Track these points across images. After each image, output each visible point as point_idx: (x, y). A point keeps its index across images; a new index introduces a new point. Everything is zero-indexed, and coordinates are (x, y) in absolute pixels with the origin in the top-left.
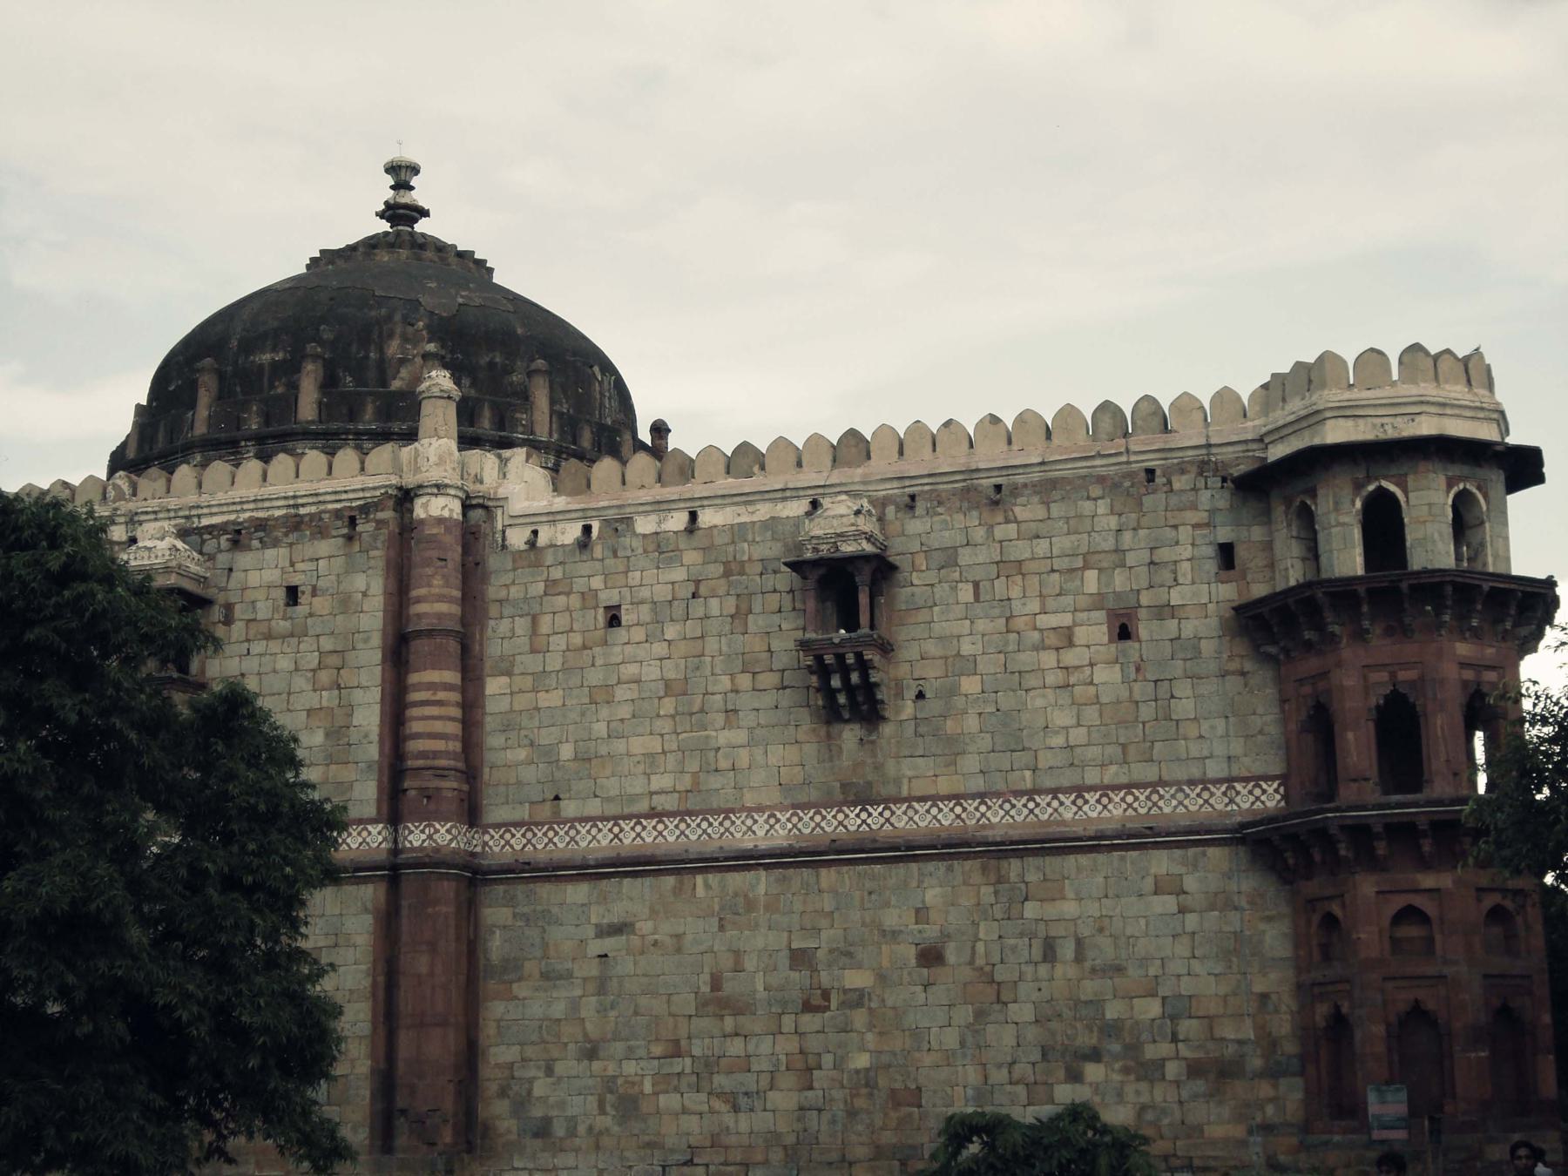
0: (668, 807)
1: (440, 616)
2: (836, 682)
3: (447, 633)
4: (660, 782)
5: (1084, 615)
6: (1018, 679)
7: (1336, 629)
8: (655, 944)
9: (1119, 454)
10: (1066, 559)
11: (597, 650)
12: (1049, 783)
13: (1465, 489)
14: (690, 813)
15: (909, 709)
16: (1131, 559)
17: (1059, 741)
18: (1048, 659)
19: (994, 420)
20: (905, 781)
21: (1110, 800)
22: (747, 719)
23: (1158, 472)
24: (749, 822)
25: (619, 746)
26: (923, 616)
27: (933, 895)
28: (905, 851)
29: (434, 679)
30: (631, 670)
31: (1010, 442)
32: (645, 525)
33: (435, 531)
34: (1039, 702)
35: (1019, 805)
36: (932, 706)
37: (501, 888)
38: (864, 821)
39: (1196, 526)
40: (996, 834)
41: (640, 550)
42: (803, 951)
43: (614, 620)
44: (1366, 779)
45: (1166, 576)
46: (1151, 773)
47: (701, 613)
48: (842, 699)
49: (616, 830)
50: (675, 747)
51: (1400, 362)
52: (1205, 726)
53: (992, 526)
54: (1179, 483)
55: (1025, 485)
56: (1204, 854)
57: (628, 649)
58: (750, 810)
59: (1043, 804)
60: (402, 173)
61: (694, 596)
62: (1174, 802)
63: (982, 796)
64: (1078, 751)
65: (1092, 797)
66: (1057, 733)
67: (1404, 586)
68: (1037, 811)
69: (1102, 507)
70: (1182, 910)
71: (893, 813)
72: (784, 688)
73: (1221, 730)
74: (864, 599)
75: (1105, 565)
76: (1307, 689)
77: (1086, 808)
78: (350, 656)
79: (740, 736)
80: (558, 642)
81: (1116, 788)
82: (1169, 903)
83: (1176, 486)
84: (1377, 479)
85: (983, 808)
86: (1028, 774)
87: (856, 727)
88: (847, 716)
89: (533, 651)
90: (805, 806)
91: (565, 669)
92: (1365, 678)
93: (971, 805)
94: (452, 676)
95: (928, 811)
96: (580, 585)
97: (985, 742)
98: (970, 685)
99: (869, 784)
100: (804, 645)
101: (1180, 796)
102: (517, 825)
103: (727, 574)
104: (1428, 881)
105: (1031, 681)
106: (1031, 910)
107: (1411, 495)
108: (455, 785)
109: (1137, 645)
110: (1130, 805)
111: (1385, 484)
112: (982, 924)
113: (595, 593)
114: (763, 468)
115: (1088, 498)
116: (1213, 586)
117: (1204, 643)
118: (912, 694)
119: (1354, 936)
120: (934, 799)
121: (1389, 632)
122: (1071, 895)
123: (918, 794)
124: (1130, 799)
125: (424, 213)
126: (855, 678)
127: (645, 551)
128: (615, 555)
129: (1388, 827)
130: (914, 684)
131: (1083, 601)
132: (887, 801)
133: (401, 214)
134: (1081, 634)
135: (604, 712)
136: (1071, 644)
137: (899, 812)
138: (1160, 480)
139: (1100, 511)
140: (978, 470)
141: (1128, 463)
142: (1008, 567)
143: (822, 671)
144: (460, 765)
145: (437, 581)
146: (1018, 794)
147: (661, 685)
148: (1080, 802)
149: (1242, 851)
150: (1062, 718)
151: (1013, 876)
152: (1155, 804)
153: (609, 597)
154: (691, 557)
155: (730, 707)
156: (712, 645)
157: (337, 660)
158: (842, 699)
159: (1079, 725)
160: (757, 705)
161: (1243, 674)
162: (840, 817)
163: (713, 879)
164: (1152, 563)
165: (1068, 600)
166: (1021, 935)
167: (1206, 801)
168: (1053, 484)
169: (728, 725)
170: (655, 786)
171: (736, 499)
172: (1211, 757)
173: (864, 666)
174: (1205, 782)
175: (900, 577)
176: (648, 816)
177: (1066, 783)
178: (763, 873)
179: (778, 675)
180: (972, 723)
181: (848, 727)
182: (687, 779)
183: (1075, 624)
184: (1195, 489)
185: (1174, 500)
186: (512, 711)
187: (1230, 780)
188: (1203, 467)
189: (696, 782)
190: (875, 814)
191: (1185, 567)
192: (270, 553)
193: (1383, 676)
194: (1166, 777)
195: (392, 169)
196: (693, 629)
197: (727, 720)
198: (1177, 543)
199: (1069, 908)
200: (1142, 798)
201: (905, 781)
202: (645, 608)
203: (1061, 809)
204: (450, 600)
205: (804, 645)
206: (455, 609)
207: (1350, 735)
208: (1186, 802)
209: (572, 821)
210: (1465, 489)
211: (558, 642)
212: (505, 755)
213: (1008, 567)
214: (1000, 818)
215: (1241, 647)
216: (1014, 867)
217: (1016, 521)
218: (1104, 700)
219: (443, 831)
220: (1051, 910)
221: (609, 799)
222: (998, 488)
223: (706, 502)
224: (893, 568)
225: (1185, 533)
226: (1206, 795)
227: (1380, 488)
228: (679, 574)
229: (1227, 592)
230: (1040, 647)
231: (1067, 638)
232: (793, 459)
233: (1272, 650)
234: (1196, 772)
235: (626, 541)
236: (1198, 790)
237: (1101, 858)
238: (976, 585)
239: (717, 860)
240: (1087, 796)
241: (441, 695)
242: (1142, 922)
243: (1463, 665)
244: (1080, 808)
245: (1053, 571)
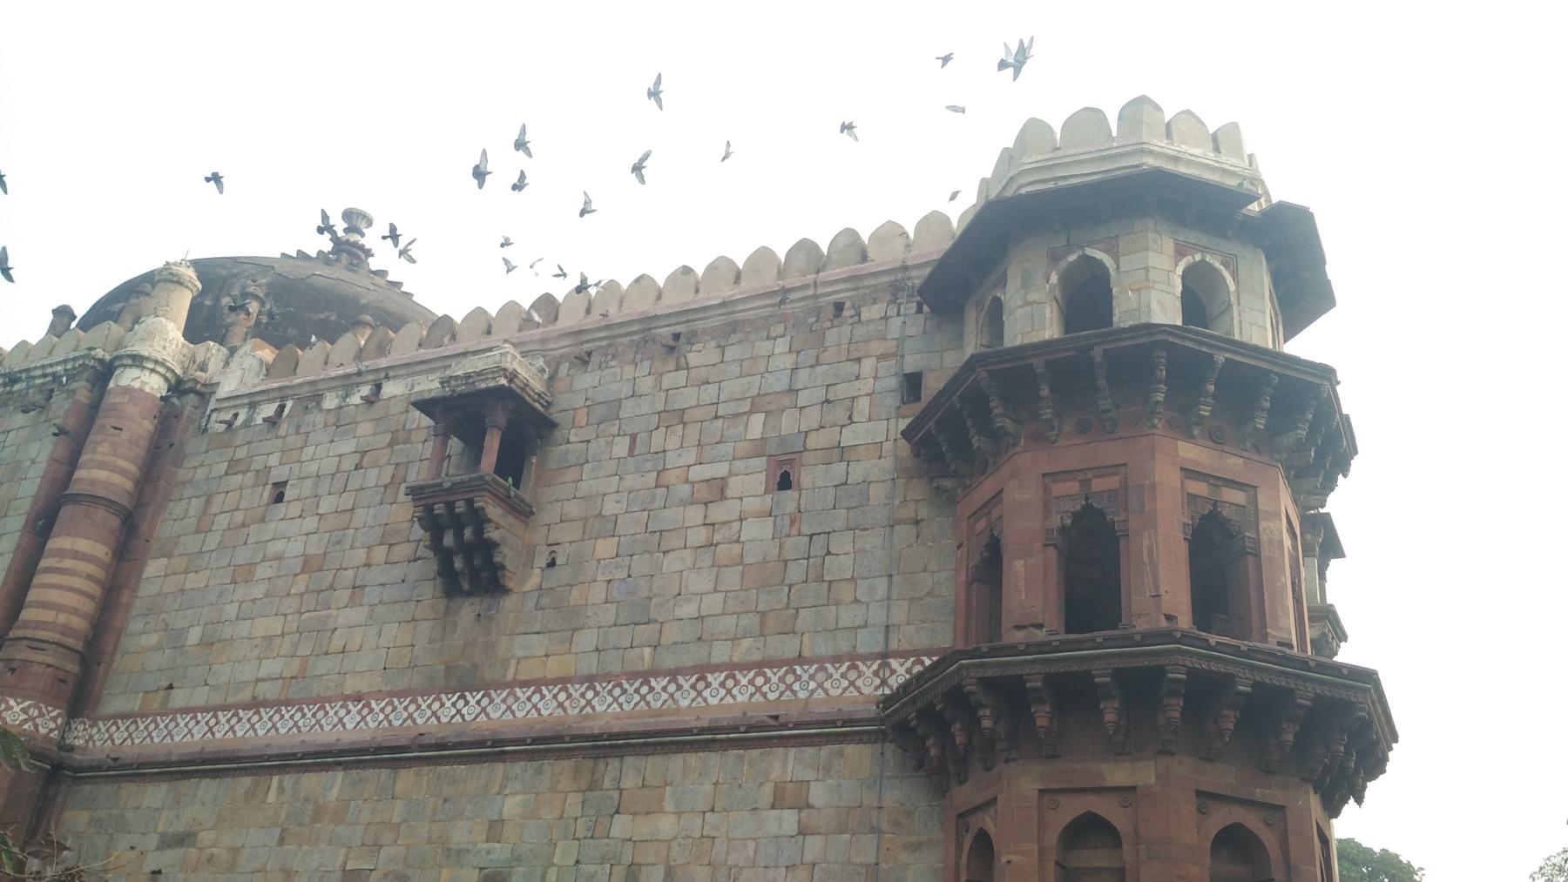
0: (270, 696)
1: (93, 482)
2: (448, 540)
3: (109, 503)
4: (271, 667)
5: (739, 465)
6: (658, 540)
7: (1009, 425)
8: (210, 859)
9: (805, 287)
10: (733, 404)
12: (670, 662)
13: (1203, 261)
14: (288, 703)
15: (534, 579)
16: (803, 399)
17: (687, 610)
18: (695, 514)
19: (686, 270)
20: (514, 662)
21: (737, 683)
22: (372, 595)
23: (848, 304)
24: (342, 712)
25: (244, 628)
26: (571, 475)
27: (511, 806)
28: (490, 749)
29: (80, 550)
30: (276, 547)
31: (697, 291)
32: (330, 402)
33: (118, 400)
34: (677, 566)
35: (631, 690)
36: (562, 574)
37: (87, 788)
38: (459, 711)
39: (880, 358)
40: (595, 727)
42: (356, 872)
43: (279, 498)
44: (1039, 626)
45: (840, 415)
46: (789, 647)
47: (357, 486)
48: (458, 564)
49: (213, 722)
50: (295, 626)
51: (1121, 117)
52: (863, 586)
53: (661, 375)
54: (871, 312)
55: (704, 331)
56: (841, 754)
57: (283, 524)
58: (346, 698)
59: (658, 688)
61: (357, 467)
62: (813, 685)
63: (591, 680)
64: (710, 621)
65: (715, 679)
66: (688, 601)
67: (1097, 354)
68: (649, 698)
69: (781, 345)
70: (803, 832)
71: (492, 701)
73: (881, 592)
74: (493, 443)
75: (773, 407)
76: (981, 524)
77: (706, 693)
79: (357, 614)
80: (222, 522)
81: (745, 667)
82: (789, 820)
83: (865, 316)
84: (1082, 248)
85: (590, 695)
86: (648, 651)
87: (475, 600)
88: (466, 587)
89: (198, 531)
90: (401, 694)
91: (221, 546)
92: (1046, 490)
93: (576, 690)
94: (102, 551)
95: (529, 699)
96: (258, 464)
97: (609, 614)
98: (605, 548)
99: (476, 666)
100: (415, 492)
101: (821, 676)
102: (124, 717)
103: (391, 444)
104: (1117, 774)
105: (672, 541)
106: (621, 826)
107: (1123, 260)
108: (50, 660)
109: (796, 495)
110: (758, 689)
111: (1089, 252)
112: (560, 843)
113: (268, 469)
114: (453, 337)
115: (768, 338)
116: (893, 421)
117: (873, 489)
118: (541, 561)
119: (1004, 860)
120: (538, 684)
121: (1083, 428)
122: (669, 805)
123: (522, 677)
124: (760, 681)
126: (468, 533)
127: (326, 426)
128: (298, 427)
129: (1050, 679)
130: (546, 551)
131: (743, 448)
132: (486, 687)
134: (735, 486)
135: (241, 592)
136: (723, 496)
137: (498, 700)
138: (846, 313)
139: (777, 351)
140: (656, 317)
141: (815, 297)
142: (675, 417)
143: (433, 524)
144: (79, 646)
145: (104, 448)
146: (631, 676)
147: (300, 561)
148: (701, 685)
149: (890, 748)
150: (698, 582)
151: (607, 784)
152: (789, 687)
153: (278, 474)
154: (365, 429)
155: (359, 582)
156: (360, 516)
158: (458, 564)
159: (715, 591)
160: (383, 580)
161: (917, 522)
162: (436, 705)
163: (289, 780)
164: (827, 401)
165: (727, 448)
166: (603, 860)
167: (852, 683)
168: (734, 327)
169: (352, 603)
170: (263, 673)
171: (419, 368)
172: (865, 626)
173: (479, 519)
174: (854, 658)
175: (557, 434)
176: (246, 707)
177: (688, 661)
178: (340, 775)
180: (598, 593)
182: (297, 661)
183: (731, 474)
184: (886, 318)
185: (860, 331)
186: (160, 594)
187: (885, 656)
188: (896, 289)
189: (304, 668)
190: (473, 702)
191: (863, 403)
193: (1073, 487)
194: (806, 653)
196: (347, 500)
197: (352, 597)
198: (858, 378)
199: (666, 825)
200: (775, 679)
201: (514, 662)
202: (309, 482)
203: (677, 695)
204: (123, 472)
205: (415, 492)
206: (128, 485)
207: (1019, 565)
208: (827, 685)
209: (175, 712)
210: (1203, 261)
211: (222, 522)
212: (140, 639)
213: (675, 417)
214: (608, 708)
215: (918, 489)
216: (610, 769)
217: (688, 368)
218: (748, 560)
219: (17, 709)
220: (643, 828)
221: (217, 688)
222: (677, 337)
224: (552, 425)
225: (868, 365)
226: (853, 675)
227: (1085, 258)
228: (348, 446)
229: (904, 424)
230: (684, 503)
231: (719, 490)
232: (484, 327)
233: (948, 484)
234: (844, 646)
235: (310, 418)
236: (844, 668)
237: (714, 758)
238: (633, 438)
239: (293, 756)
240: (710, 677)
241: (69, 563)
242: (752, 845)
243: (1189, 473)
244: (699, 693)
245: (717, 417)
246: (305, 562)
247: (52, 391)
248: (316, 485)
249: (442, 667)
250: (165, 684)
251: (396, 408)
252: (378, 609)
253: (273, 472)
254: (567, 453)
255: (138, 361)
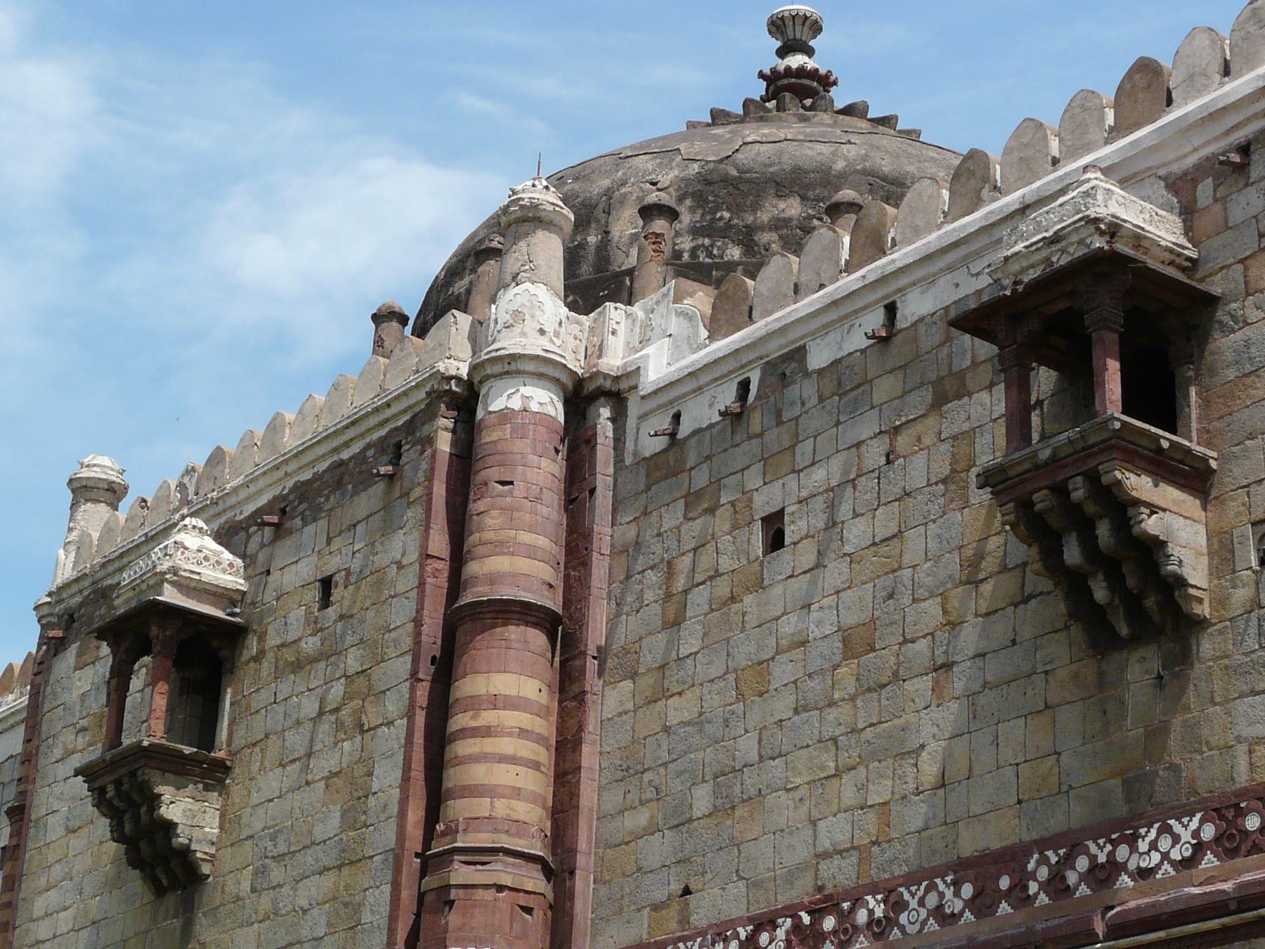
2: (1072, 554)
4: (835, 831)
11: (748, 599)
41: (815, 400)
43: (776, 541)
48: (1100, 593)
60: (792, 33)
72: (1026, 600)
78: (377, 673)
88: (1124, 631)
100: (993, 479)
125: (826, 81)
126: (1103, 531)
127: (821, 399)
133: (796, 90)
143: (1037, 529)
157: (362, 686)
158: (1100, 593)
170: (825, 844)
179: (1017, 572)
181: (1135, 656)
192: (310, 529)
195: (777, 25)
196: (885, 521)
202: (819, 503)
205: (993, 479)
223: (903, 281)
224: (1211, 301)
228: (866, 426)
235: (793, 392)
246: (845, 641)
247: (398, 446)
248: (832, 507)
249: (1116, 783)
250: (676, 887)
251: (930, 338)
252: (981, 700)
253: (758, 499)
254: (1247, 343)
255: (513, 367)
